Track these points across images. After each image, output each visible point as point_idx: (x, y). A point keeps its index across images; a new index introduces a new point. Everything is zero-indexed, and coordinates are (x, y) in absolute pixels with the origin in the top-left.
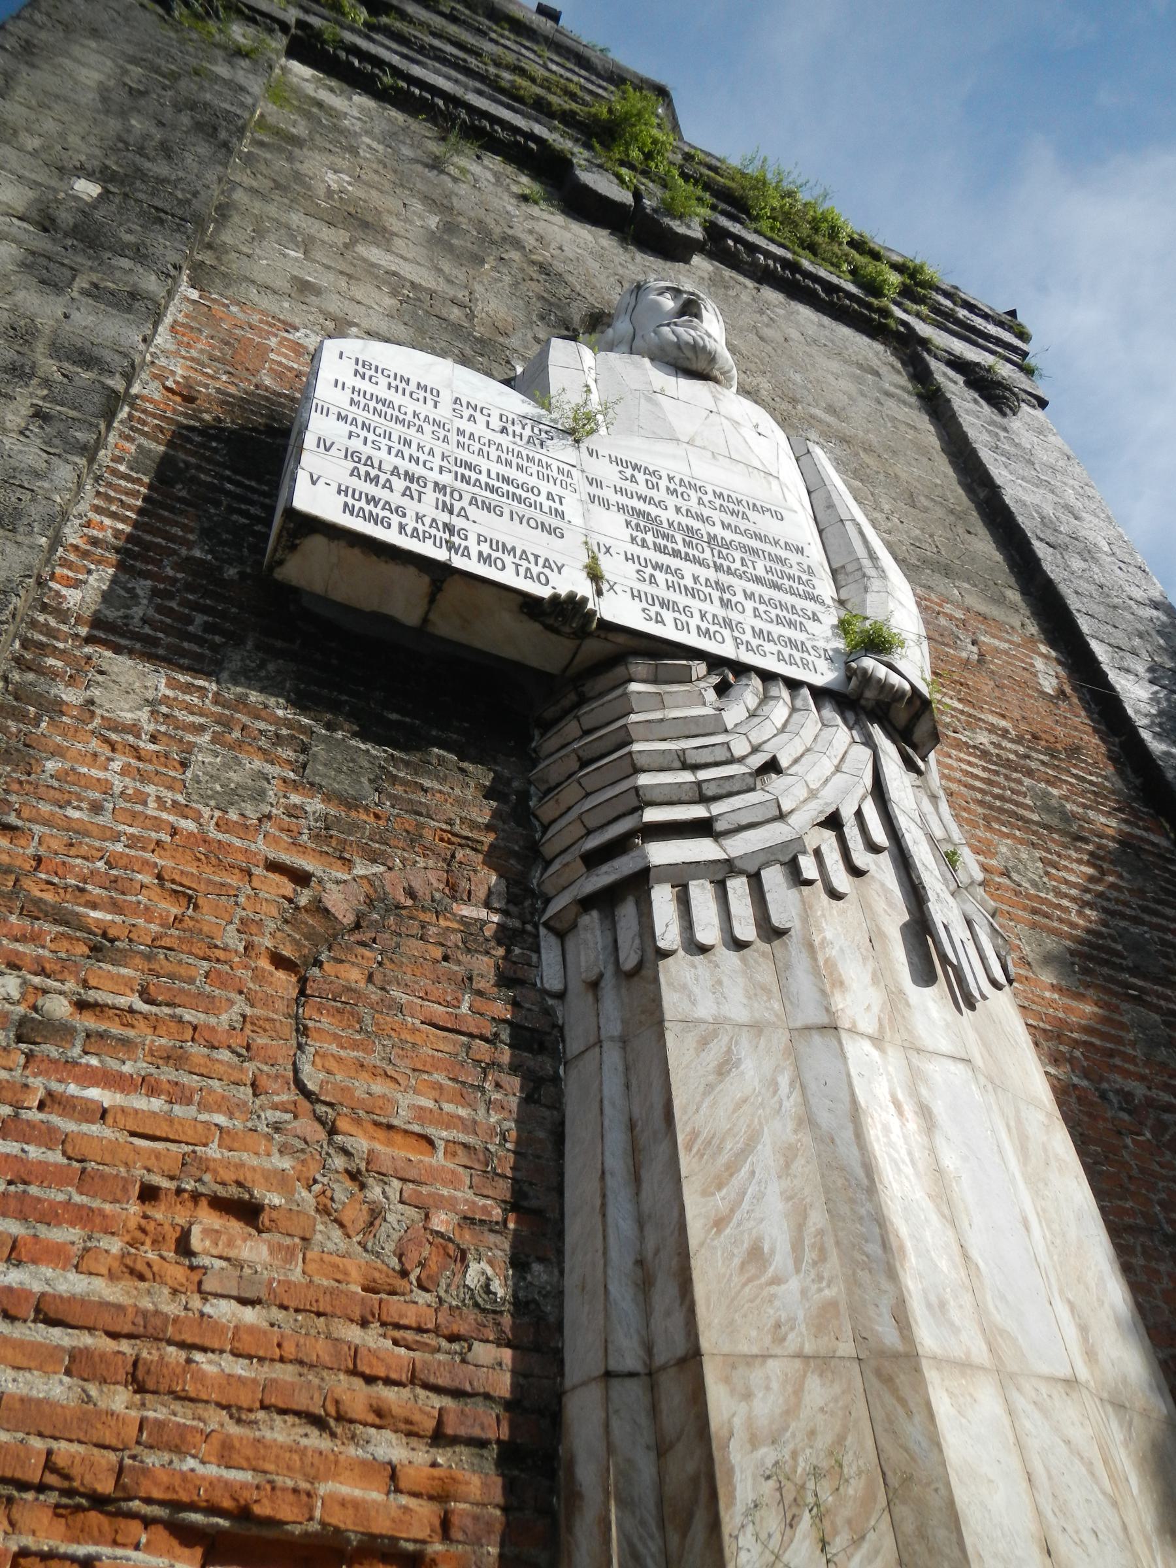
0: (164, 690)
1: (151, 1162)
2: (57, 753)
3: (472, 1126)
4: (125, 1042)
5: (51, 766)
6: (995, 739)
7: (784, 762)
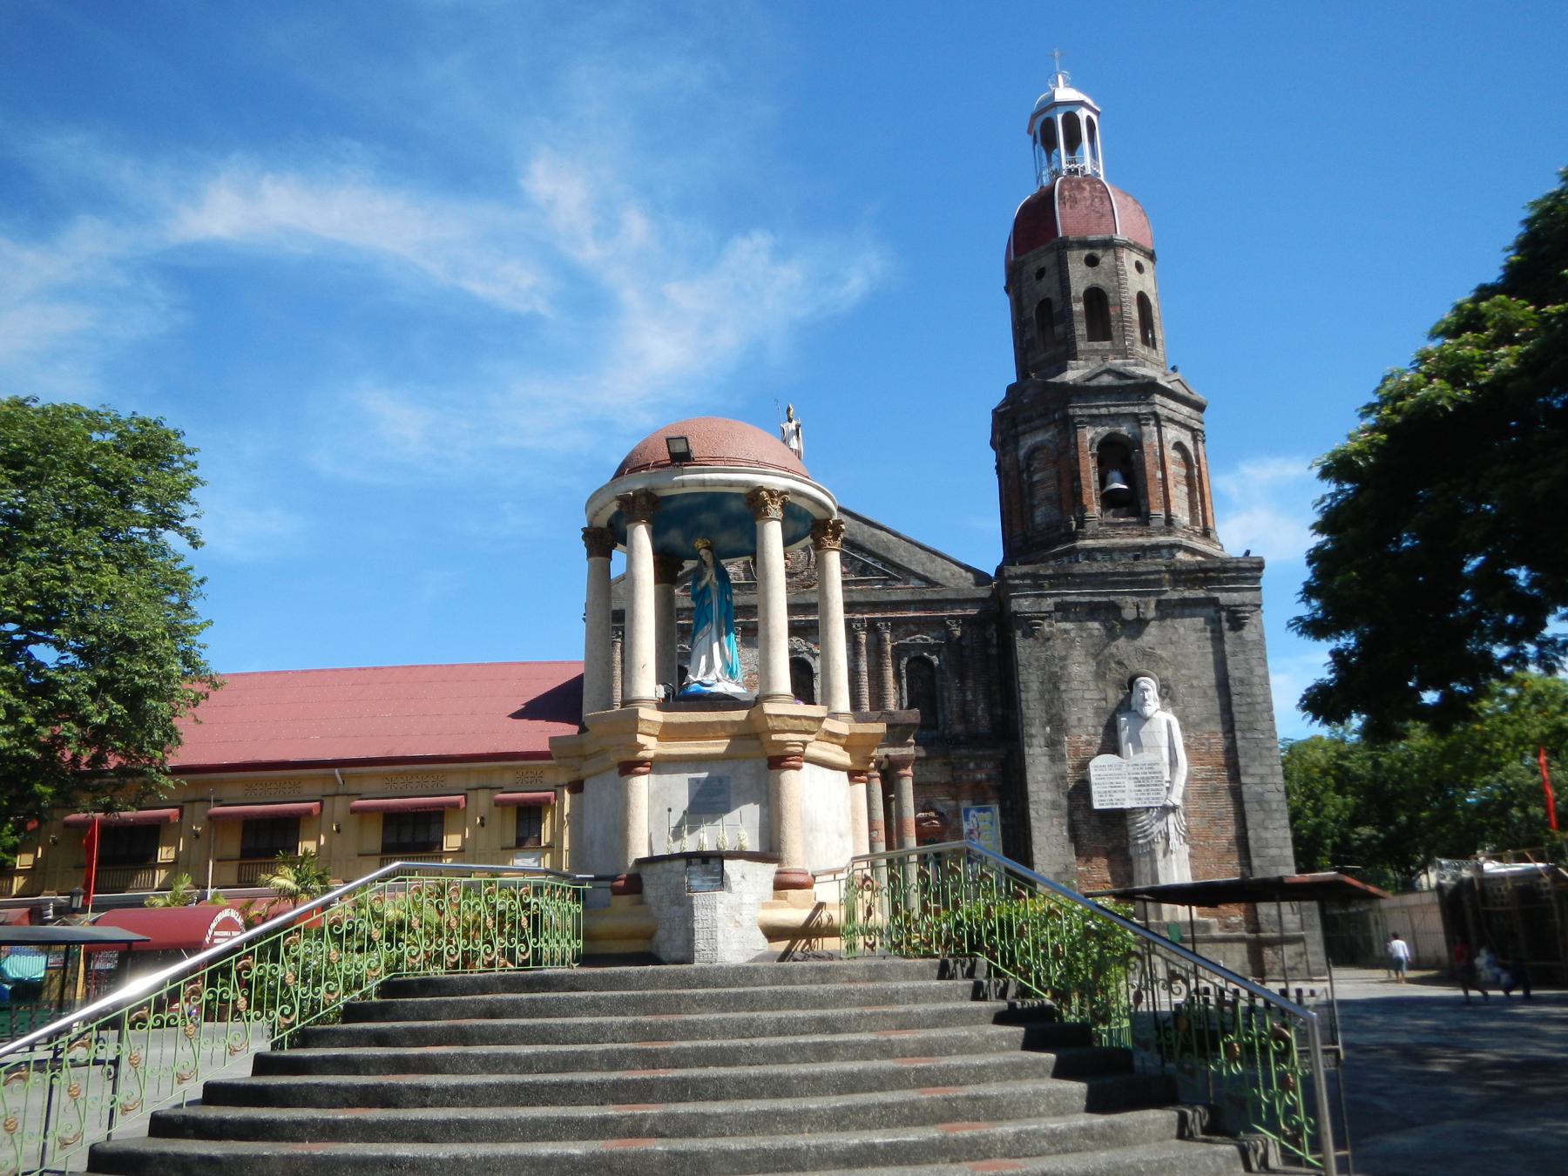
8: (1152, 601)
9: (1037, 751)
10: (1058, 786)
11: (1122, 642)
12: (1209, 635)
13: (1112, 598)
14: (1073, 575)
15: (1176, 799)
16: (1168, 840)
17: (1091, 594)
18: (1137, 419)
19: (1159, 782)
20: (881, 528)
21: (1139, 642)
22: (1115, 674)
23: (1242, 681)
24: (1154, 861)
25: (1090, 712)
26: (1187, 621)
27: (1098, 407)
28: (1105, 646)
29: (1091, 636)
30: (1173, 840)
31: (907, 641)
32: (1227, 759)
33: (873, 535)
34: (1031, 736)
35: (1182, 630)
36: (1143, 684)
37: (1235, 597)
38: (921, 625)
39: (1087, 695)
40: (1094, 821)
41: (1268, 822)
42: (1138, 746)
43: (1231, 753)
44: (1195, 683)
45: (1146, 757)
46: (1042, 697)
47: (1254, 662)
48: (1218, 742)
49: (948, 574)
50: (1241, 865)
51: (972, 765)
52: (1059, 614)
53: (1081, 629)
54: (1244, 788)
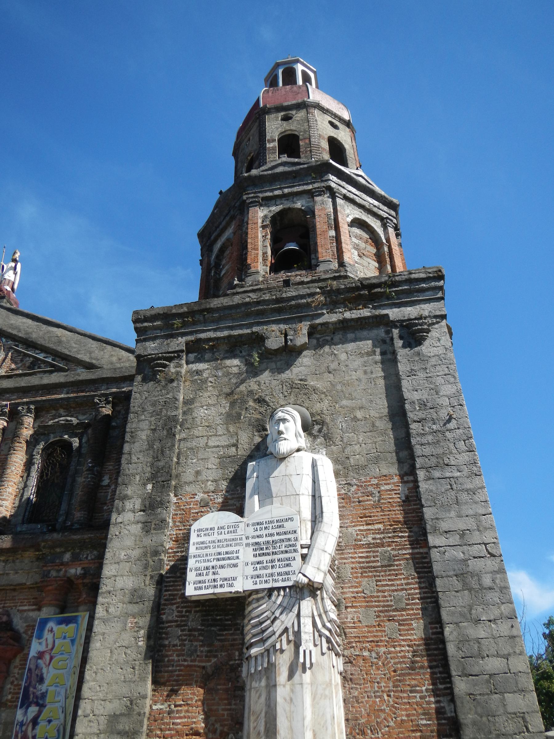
0: (180, 633)
1: (186, 729)
2: (167, 656)
3: (230, 710)
4: (181, 710)
5: (166, 659)
6: (374, 536)
7: (278, 616)
8: (304, 327)
9: (128, 516)
10: (146, 567)
11: (266, 376)
12: (378, 358)
13: (255, 329)
14: (210, 310)
15: (316, 570)
16: (297, 645)
17: (231, 328)
18: (311, 194)
19: (292, 547)
20: (58, 326)
21: (287, 375)
22: (252, 411)
23: (423, 405)
24: (272, 687)
25: (213, 462)
26: (351, 346)
27: (272, 191)
28: (243, 382)
29: (228, 374)
30: (307, 643)
31: (51, 423)
32: (406, 512)
33: (49, 332)
34: (125, 498)
35: (343, 356)
36: (280, 415)
37: (410, 312)
38: (68, 406)
39: (212, 442)
40: (194, 621)
41: (478, 610)
42: (266, 496)
43: (413, 503)
44: (359, 414)
45: (276, 511)
46: (151, 446)
47: (439, 380)
48: (393, 490)
49: (114, 359)
50: (435, 693)
51: (67, 557)
52: (192, 356)
53: (217, 369)
54: (435, 554)
